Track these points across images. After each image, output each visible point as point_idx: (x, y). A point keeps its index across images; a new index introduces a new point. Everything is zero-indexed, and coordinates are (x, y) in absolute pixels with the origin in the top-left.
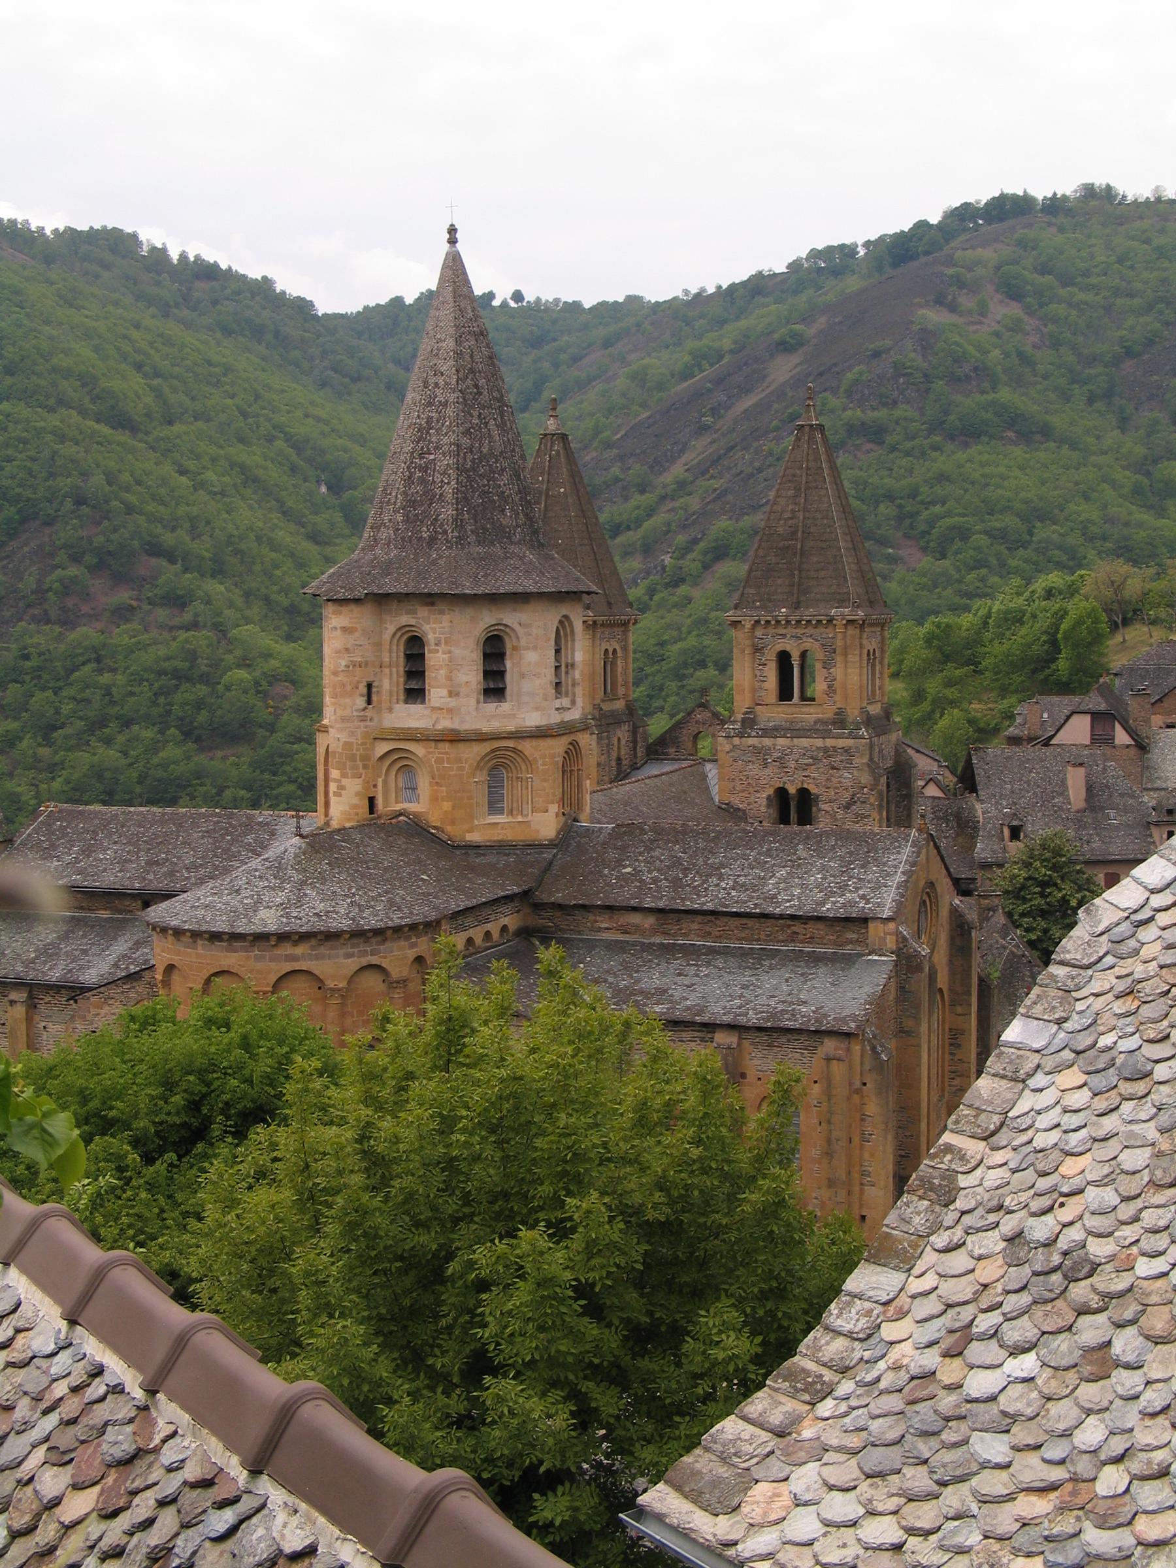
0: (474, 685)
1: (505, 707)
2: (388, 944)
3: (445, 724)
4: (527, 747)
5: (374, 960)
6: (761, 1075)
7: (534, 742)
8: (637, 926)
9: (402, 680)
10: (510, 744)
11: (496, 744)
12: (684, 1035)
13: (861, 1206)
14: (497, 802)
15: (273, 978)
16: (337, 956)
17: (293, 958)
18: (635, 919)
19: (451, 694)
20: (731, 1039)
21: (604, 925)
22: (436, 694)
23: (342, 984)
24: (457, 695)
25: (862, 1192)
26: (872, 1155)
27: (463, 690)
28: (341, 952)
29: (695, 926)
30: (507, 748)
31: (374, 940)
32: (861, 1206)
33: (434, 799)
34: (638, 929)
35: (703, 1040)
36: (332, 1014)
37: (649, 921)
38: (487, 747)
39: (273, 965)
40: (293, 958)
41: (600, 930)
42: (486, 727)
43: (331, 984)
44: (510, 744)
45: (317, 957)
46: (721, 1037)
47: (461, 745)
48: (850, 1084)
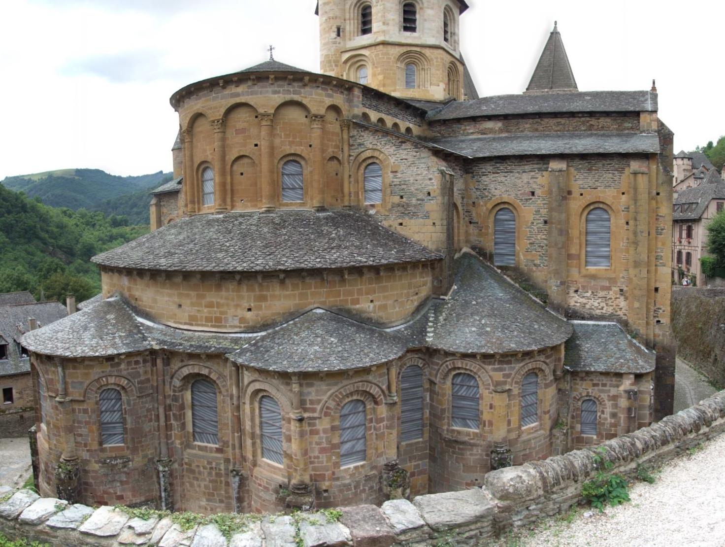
0: (397, 21)
1: (414, 34)
2: (308, 89)
3: (381, 38)
4: (427, 52)
5: (296, 97)
6: (582, 191)
7: (431, 50)
8: (491, 129)
9: (360, 26)
10: (418, 49)
11: (409, 49)
12: (526, 167)
13: (656, 281)
14: (411, 82)
15: (223, 110)
16: (267, 92)
17: (238, 95)
18: (490, 125)
19: (384, 24)
20: (562, 165)
21: (471, 131)
22: (375, 26)
23: (272, 111)
24: (388, 24)
25: (656, 271)
26: (663, 244)
27: (391, 23)
28: (270, 90)
29: (528, 126)
30: (416, 52)
31: (296, 84)
32: (656, 281)
33: (374, 75)
34: (491, 131)
35: (540, 170)
36: (264, 133)
37: (499, 125)
38: (405, 49)
39: (223, 102)
40: (238, 95)
41: (468, 134)
42: (404, 41)
43: (261, 110)
44: (418, 49)
45: (252, 93)
46: (554, 165)
47: (389, 47)
48: (649, 193)
